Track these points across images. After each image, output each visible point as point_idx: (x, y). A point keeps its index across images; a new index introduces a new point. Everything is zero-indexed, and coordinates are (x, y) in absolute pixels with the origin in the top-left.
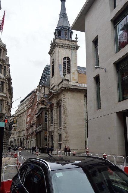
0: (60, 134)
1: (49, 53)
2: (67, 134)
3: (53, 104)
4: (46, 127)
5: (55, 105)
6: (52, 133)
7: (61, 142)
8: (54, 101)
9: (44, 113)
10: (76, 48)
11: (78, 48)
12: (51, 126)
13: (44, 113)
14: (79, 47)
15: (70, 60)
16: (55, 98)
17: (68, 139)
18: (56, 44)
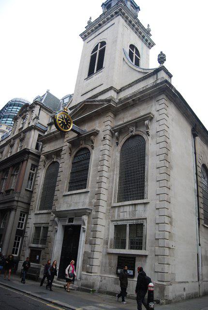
0: (135, 222)
1: (81, 35)
2: (171, 223)
3: (96, 133)
4: (26, 201)
5: (101, 135)
6: (85, 218)
7: (127, 251)
8: (104, 126)
9: (30, 163)
10: (149, 44)
11: (153, 46)
12: (65, 196)
13: (30, 163)
14: (154, 44)
15: (139, 56)
16: (109, 118)
17: (173, 244)
18: (123, 11)
